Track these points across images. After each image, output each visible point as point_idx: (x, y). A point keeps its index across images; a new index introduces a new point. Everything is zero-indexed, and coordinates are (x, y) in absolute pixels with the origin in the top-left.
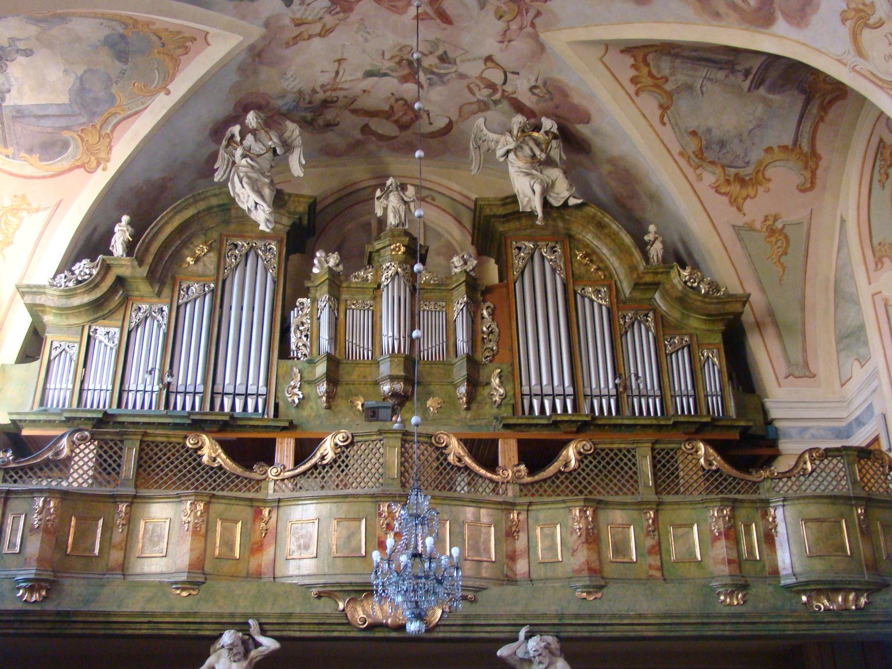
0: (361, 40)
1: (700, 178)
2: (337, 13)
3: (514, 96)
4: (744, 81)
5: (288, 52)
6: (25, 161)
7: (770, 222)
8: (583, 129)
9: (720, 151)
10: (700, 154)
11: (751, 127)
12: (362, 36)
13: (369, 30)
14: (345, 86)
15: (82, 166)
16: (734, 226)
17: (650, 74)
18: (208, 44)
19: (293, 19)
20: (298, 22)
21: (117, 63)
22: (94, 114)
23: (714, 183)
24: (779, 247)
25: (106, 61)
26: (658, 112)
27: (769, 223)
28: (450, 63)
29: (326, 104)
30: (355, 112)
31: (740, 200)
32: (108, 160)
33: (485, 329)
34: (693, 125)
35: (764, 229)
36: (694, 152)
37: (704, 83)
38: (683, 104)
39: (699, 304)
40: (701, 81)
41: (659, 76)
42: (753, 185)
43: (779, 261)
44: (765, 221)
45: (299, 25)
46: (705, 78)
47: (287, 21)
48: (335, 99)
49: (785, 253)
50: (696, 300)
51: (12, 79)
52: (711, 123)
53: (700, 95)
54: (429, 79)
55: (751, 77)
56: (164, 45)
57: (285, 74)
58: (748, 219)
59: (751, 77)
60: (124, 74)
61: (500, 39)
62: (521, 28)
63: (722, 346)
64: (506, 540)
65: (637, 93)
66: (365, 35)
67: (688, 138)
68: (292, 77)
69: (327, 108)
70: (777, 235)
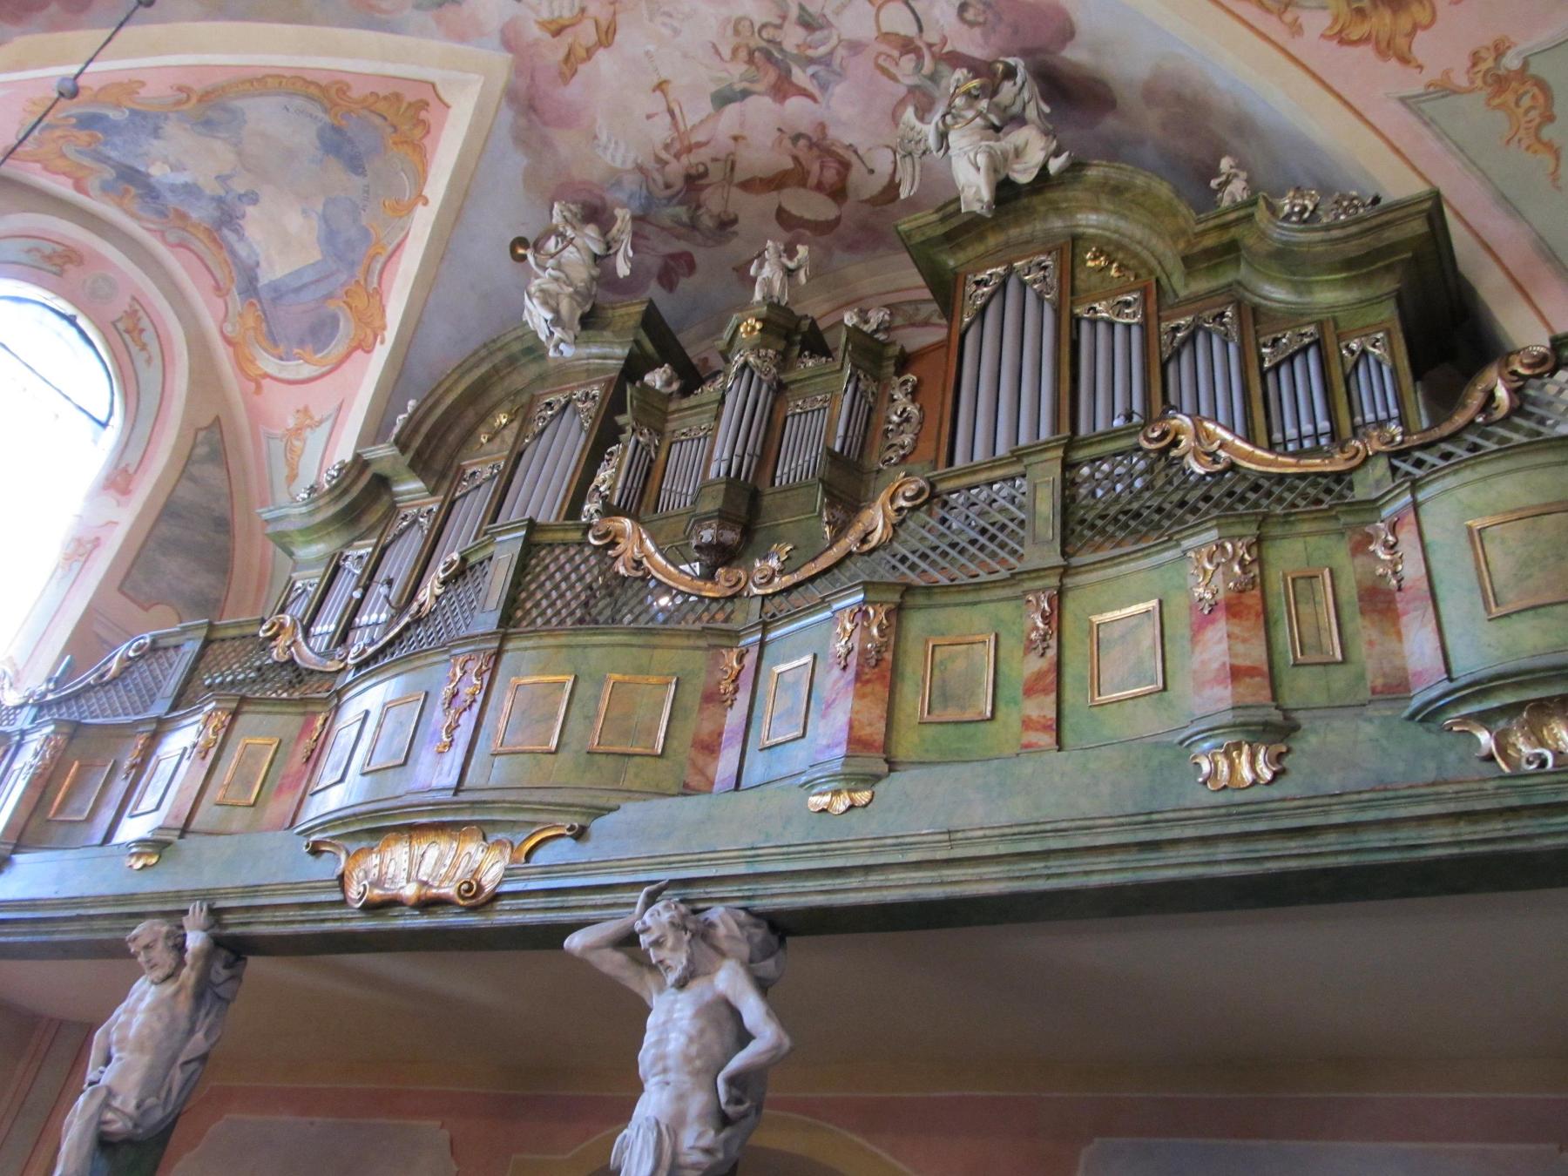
0: (667, 32)
1: (1296, 29)
3: (946, 50)
5: (573, 91)
6: (300, 359)
7: (1490, 63)
8: (1075, 54)
12: (664, 24)
13: (666, 9)
14: (699, 137)
16: (1403, 100)
18: (448, 107)
19: (543, 25)
20: (554, 27)
21: (356, 178)
22: (352, 264)
23: (1331, 28)
24: (1527, 112)
25: (337, 175)
27: (1483, 67)
28: (821, 28)
29: (694, 181)
30: (746, 185)
31: (1401, 42)
32: (384, 328)
33: (895, 418)
35: (1479, 83)
39: (1320, 249)
43: (1539, 140)
44: (1474, 65)
45: (557, 33)
47: (535, 32)
48: (701, 169)
49: (1549, 118)
50: (1310, 244)
51: (255, 247)
54: (813, 76)
57: (595, 137)
58: (1432, 73)
60: (367, 192)
63: (1396, 326)
66: (667, 20)
68: (609, 140)
69: (702, 188)
70: (1514, 84)
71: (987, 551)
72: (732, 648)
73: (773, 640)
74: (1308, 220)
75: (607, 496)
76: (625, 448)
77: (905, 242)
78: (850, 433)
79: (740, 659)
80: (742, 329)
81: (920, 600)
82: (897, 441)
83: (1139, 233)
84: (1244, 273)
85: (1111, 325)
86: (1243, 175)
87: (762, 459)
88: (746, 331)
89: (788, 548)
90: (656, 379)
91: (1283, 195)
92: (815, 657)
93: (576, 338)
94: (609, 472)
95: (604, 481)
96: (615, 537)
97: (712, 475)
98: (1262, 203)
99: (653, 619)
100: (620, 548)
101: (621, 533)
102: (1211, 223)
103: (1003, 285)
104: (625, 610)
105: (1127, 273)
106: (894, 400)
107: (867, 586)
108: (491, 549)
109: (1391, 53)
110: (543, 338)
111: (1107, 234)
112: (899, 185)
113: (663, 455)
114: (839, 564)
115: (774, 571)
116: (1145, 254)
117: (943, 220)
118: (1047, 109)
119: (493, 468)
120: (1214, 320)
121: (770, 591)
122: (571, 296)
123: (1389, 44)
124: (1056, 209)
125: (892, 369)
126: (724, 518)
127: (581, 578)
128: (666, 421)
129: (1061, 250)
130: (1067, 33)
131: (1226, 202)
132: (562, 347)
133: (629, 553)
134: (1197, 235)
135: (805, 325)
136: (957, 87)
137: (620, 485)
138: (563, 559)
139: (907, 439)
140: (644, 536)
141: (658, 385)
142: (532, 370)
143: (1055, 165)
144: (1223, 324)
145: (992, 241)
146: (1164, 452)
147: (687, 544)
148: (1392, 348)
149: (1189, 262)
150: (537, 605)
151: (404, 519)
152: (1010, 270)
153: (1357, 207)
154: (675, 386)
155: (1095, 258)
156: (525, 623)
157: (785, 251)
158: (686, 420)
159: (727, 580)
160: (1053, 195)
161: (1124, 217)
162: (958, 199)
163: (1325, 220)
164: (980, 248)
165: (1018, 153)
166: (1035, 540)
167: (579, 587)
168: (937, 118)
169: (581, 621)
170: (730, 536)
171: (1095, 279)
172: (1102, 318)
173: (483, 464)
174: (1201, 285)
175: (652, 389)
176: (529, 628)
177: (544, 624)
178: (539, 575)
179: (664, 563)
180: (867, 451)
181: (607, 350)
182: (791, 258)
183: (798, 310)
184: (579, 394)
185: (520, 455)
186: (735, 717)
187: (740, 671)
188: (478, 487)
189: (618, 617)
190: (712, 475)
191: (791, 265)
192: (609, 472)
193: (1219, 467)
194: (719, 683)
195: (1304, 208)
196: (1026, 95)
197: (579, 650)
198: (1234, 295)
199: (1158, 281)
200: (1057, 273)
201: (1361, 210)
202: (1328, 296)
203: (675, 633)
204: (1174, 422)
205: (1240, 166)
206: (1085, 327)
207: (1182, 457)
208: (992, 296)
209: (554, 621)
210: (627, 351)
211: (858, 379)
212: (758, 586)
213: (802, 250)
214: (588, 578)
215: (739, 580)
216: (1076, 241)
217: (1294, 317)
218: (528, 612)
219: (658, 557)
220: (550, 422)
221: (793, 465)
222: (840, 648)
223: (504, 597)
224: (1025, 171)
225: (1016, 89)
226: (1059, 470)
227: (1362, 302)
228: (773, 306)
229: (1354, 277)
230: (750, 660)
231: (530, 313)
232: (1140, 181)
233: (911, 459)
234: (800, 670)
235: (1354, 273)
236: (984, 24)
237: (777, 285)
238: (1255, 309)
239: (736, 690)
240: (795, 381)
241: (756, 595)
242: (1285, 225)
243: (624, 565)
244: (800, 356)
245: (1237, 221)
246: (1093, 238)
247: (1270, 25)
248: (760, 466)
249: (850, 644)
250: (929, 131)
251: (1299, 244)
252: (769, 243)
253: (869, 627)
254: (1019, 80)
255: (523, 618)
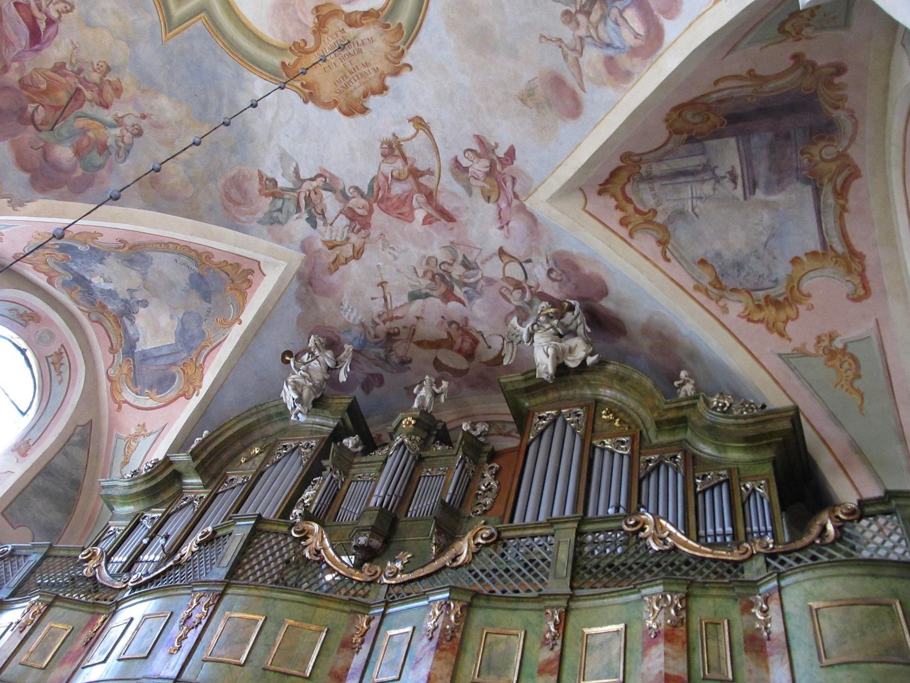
0: (391, 257)
1: (725, 310)
2: (359, 231)
3: (539, 290)
4: (735, 188)
5: (335, 278)
6: (148, 396)
7: (826, 343)
8: (607, 304)
9: (738, 276)
10: (717, 283)
11: (764, 239)
12: (390, 253)
15: (184, 395)
16: (780, 355)
17: (637, 211)
18: (265, 275)
19: (325, 242)
20: (330, 244)
23: (743, 312)
24: (846, 371)
25: (195, 300)
26: (659, 249)
27: (823, 344)
28: (473, 269)
29: (391, 336)
30: (420, 344)
31: (780, 325)
32: (200, 387)
33: (483, 488)
34: (700, 253)
35: (821, 352)
36: (710, 284)
37: (694, 204)
38: (682, 233)
40: (690, 203)
41: (646, 210)
42: (791, 306)
43: (852, 386)
44: (818, 342)
45: (331, 248)
46: (692, 198)
47: (319, 245)
48: (396, 330)
49: (858, 376)
50: (728, 425)
51: (139, 329)
52: (718, 246)
53: (696, 219)
54: (465, 292)
55: (740, 181)
56: (233, 282)
57: (342, 304)
59: (740, 181)
60: (209, 312)
61: (499, 225)
62: (509, 205)
63: (773, 477)
64: (338, 652)
65: (631, 235)
66: (392, 251)
67: (698, 269)
68: (349, 307)
70: (839, 356)
71: (526, 578)
72: (364, 614)
73: (390, 614)
74: (727, 412)
75: (307, 506)
76: (324, 479)
77: (503, 388)
78: (456, 493)
79: (368, 623)
80: (403, 422)
81: (482, 602)
82: (483, 501)
83: (633, 404)
84: (689, 435)
85: (612, 453)
86: (692, 381)
87: (403, 500)
88: (406, 424)
89: (409, 556)
90: (349, 442)
91: (713, 396)
92: (414, 628)
93: (308, 411)
94: (312, 492)
95: (308, 497)
96: (308, 533)
97: (372, 504)
98: (701, 398)
99: (320, 588)
100: (309, 541)
101: (311, 532)
102: (673, 405)
103: (554, 422)
104: (305, 580)
105: (624, 425)
106: (484, 477)
107: (452, 589)
108: (232, 528)
109: (774, 330)
110: (290, 408)
111: (615, 402)
112: (504, 357)
113: (345, 487)
114: (437, 572)
115: (398, 569)
116: (635, 416)
117: (525, 380)
118: (589, 330)
119: (244, 478)
120: (671, 459)
121: (393, 582)
122: (310, 387)
123: (774, 324)
124: (590, 386)
125: (485, 459)
126: (374, 531)
127: (282, 556)
128: (351, 468)
129: (589, 406)
130: (604, 292)
131: (682, 395)
132: (300, 415)
133: (313, 545)
134: (664, 410)
135: (440, 426)
136: (542, 311)
137: (316, 501)
138: (273, 542)
139: (488, 501)
140: (325, 536)
141: (350, 446)
142: (280, 425)
143: (590, 360)
144: (676, 462)
145: (552, 395)
146: (636, 533)
147: (350, 544)
148: (769, 490)
149: (659, 425)
150: (252, 568)
151: (185, 500)
152: (559, 414)
153: (752, 409)
154: (360, 448)
155: (607, 414)
156: (242, 578)
157: (435, 383)
158: (363, 469)
159: (369, 571)
160: (586, 376)
161: (625, 394)
162: (535, 370)
163: (735, 413)
164: (544, 399)
165: (571, 351)
166: (555, 576)
167: (279, 561)
168: (529, 325)
169: (276, 582)
170: (376, 543)
171: (606, 425)
172: (608, 448)
173: (238, 476)
174: (665, 438)
175: (347, 448)
176: (244, 582)
177: (254, 580)
178: (257, 549)
179: (333, 554)
180: (464, 504)
181: (324, 421)
182: (438, 387)
183: (437, 416)
184: (304, 443)
185: (262, 474)
186: (358, 660)
187: (367, 630)
188: (233, 488)
189: (299, 584)
190: (372, 504)
191: (437, 391)
192: (312, 492)
193: (667, 547)
194: (353, 636)
195: (724, 405)
196: (579, 321)
197: (271, 601)
198: (683, 446)
199: (641, 432)
200: (585, 420)
201: (755, 411)
202: (735, 455)
203: (332, 599)
204: (643, 517)
205: (691, 376)
206: (597, 452)
207: (646, 539)
208: (547, 426)
209: (260, 580)
210: (336, 423)
211: (465, 462)
212: (387, 578)
213: (445, 384)
214: (286, 557)
215: (377, 572)
216: (597, 403)
217: (715, 464)
218: (246, 571)
219: (330, 550)
220: (283, 457)
221: (420, 506)
222: (430, 625)
223: (233, 560)
224: (573, 361)
225: (573, 317)
226: (574, 536)
227: (754, 461)
228: (423, 411)
229: (750, 447)
230: (374, 624)
231: (285, 393)
232: (636, 376)
233: (489, 513)
234: (404, 635)
235: (751, 444)
236: (560, 281)
237: (428, 400)
238: (694, 457)
239: (362, 642)
240: (428, 457)
241: (385, 584)
242: (714, 413)
243: (309, 552)
244: (434, 443)
245: (688, 406)
246: (607, 403)
247: (712, 305)
248: (400, 504)
249: (436, 624)
250: (524, 331)
251: (720, 424)
252: (427, 377)
253: (449, 615)
254: (576, 313)
255: (242, 575)
